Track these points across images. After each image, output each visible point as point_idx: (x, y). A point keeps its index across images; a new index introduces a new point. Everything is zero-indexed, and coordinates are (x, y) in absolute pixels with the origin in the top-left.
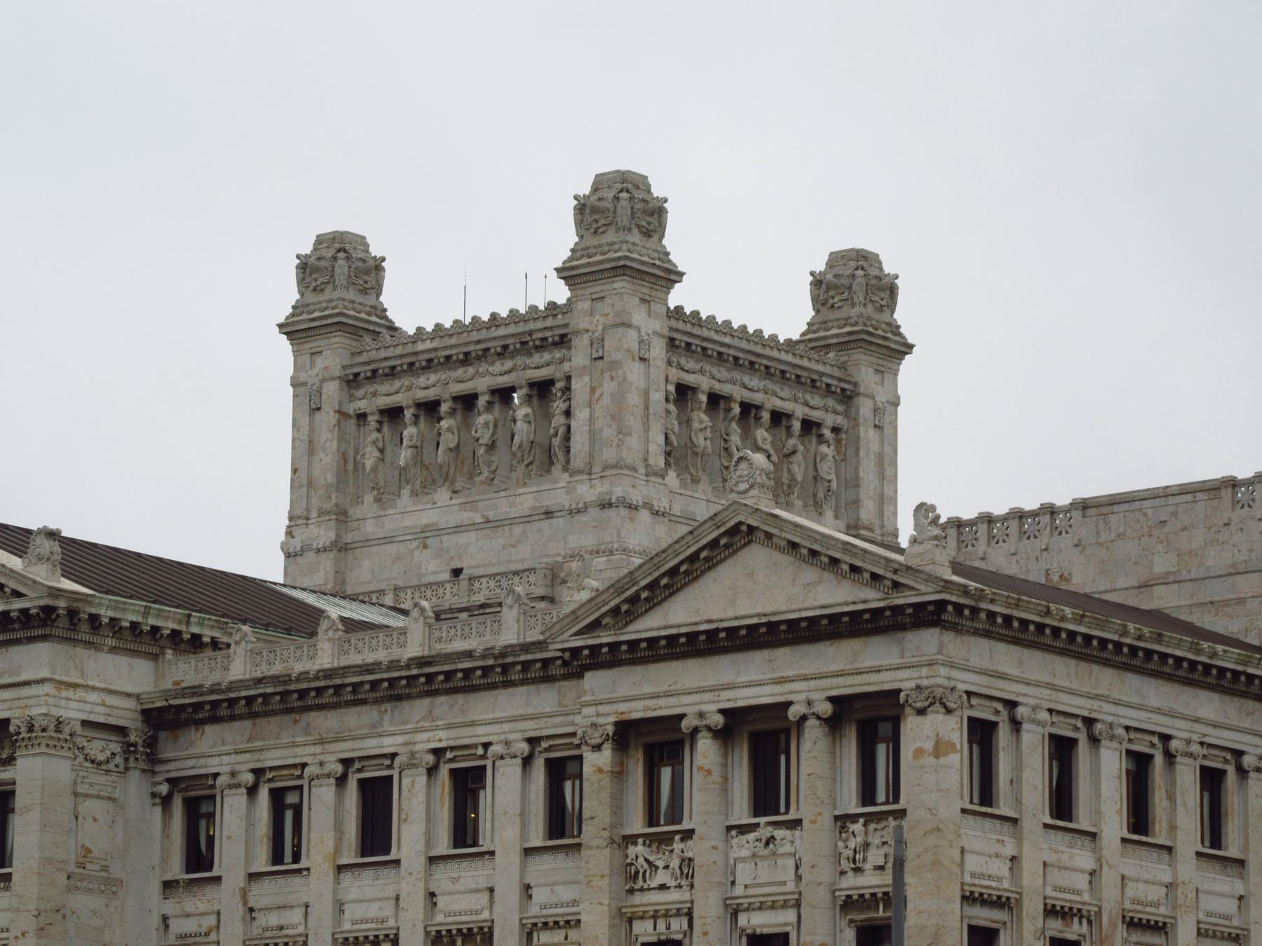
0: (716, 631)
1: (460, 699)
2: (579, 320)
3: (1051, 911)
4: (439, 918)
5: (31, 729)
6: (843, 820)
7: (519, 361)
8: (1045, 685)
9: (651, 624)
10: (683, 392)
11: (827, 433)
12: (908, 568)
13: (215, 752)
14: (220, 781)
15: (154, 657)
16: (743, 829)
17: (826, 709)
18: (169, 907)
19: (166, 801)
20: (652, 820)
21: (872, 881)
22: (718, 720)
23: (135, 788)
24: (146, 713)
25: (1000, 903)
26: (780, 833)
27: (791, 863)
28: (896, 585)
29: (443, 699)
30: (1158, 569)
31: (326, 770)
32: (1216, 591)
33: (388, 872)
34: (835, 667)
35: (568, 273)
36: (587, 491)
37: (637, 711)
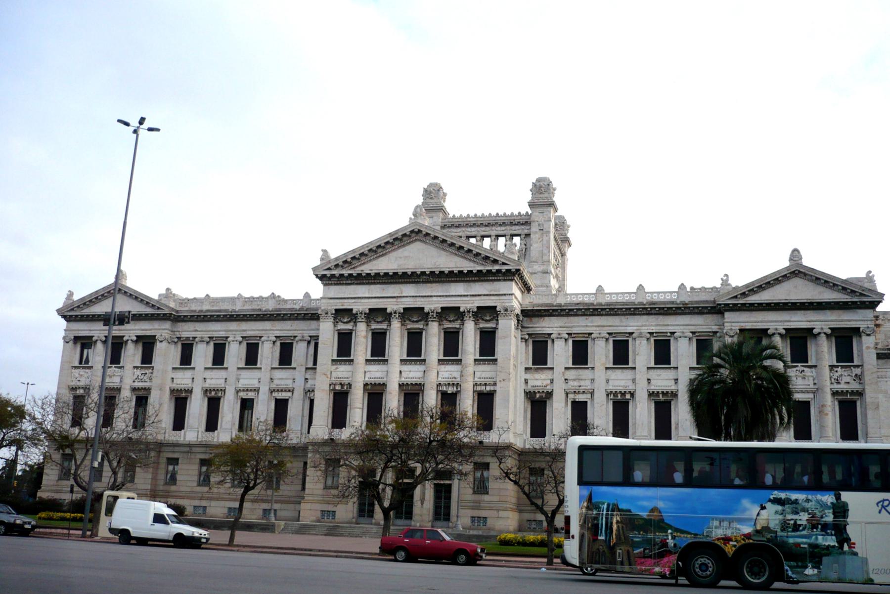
1: (661, 317)
4: (653, 387)
5: (506, 310)
6: (832, 367)
7: (508, 227)
12: (870, 290)
14: (552, 336)
15: (523, 293)
18: (528, 376)
19: (526, 341)
22: (784, 332)
26: (806, 369)
28: (861, 295)
31: (602, 335)
33: (629, 372)
35: (532, 205)
36: (537, 268)
37: (749, 326)
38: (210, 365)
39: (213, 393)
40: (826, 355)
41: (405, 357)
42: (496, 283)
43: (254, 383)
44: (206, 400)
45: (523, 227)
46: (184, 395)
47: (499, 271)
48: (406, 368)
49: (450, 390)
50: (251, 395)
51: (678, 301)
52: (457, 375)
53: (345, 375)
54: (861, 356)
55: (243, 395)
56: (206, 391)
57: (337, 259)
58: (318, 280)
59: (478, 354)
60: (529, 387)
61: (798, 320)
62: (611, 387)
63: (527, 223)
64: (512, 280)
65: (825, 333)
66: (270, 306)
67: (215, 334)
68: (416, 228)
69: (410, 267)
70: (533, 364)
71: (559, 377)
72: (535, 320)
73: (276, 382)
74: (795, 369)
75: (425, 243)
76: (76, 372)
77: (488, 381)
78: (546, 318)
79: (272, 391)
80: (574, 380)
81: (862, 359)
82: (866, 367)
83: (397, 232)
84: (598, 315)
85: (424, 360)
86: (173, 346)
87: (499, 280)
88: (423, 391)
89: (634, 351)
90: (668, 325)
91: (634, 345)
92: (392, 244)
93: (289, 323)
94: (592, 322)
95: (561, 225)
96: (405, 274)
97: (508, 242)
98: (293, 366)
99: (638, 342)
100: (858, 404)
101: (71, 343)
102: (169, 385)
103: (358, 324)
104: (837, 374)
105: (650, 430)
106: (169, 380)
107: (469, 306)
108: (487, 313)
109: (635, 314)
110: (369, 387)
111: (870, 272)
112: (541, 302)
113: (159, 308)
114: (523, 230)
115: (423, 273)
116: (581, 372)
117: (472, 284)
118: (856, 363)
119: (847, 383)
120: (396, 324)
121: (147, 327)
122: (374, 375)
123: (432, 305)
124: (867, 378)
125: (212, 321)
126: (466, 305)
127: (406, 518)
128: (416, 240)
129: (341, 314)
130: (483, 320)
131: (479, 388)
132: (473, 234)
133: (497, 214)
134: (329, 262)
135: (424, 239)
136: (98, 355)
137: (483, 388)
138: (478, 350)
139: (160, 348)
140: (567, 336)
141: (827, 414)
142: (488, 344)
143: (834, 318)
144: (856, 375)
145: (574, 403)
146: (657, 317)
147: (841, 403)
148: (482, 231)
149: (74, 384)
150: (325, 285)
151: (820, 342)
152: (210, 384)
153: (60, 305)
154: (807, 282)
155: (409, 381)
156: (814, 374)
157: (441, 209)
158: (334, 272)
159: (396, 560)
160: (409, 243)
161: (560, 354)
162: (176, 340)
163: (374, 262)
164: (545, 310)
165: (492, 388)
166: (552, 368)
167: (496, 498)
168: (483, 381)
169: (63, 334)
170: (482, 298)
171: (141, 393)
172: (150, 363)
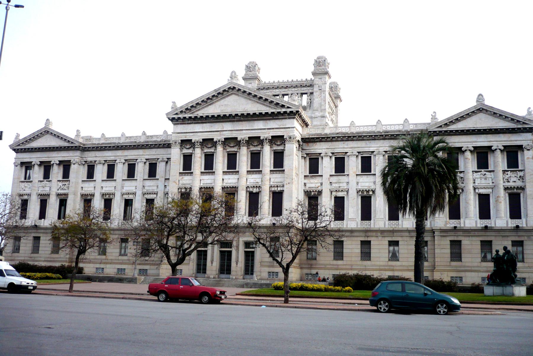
2: (315, 82)
5: (290, 138)
6: (504, 171)
7: (299, 89)
12: (529, 120)
14: (322, 155)
15: (302, 127)
16: (476, 172)
17: (502, 148)
18: (306, 181)
19: (305, 158)
22: (472, 149)
26: (487, 173)
27: (491, 179)
28: (524, 123)
29: (387, 140)
31: (354, 154)
33: (372, 177)
35: (314, 74)
36: (318, 114)
38: (105, 178)
39: (107, 196)
40: (501, 164)
41: (226, 170)
42: (284, 120)
43: (133, 189)
44: (103, 200)
45: (309, 88)
46: (89, 198)
47: (285, 112)
48: (226, 177)
49: (255, 190)
50: (131, 197)
51: (403, 130)
52: (259, 180)
53: (188, 182)
54: (524, 164)
55: (126, 197)
56: (103, 195)
57: (181, 107)
58: (170, 122)
59: (272, 167)
60: (307, 188)
61: (482, 141)
62: (360, 187)
63: (311, 86)
64: (294, 118)
65: (500, 149)
66: (142, 140)
67: (108, 159)
68: (232, 86)
69: (228, 111)
70: (310, 173)
71: (327, 182)
72: (310, 144)
73: (146, 188)
74: (480, 173)
75: (238, 95)
76: (23, 185)
77: (279, 184)
78: (318, 143)
79: (144, 194)
80: (336, 183)
81: (524, 166)
82: (526, 171)
83: (219, 89)
84: (351, 140)
85: (238, 172)
86: (82, 167)
87: (286, 118)
88: (237, 191)
89: (375, 164)
91: (375, 160)
92: (217, 96)
93: (154, 150)
94: (347, 145)
95: (334, 88)
96: (225, 115)
97: (300, 98)
98: (157, 178)
99: (377, 157)
100: (522, 195)
101: (19, 166)
102: (79, 192)
103: (196, 149)
104: (507, 176)
105: (385, 215)
106: (80, 188)
107: (266, 136)
108: (278, 140)
109: (375, 139)
110: (203, 190)
111: (530, 108)
112: (314, 133)
113: (72, 143)
115: (237, 115)
116: (340, 177)
117: (268, 121)
118: (520, 168)
119: (514, 181)
120: (220, 148)
121: (65, 155)
122: (206, 182)
123: (243, 136)
124: (527, 178)
125: (106, 150)
126: (264, 135)
127: (227, 274)
128: (232, 94)
129: (185, 143)
130: (275, 144)
131: (273, 189)
132: (277, 93)
133: (292, 80)
134: (177, 109)
135: (237, 93)
136: (37, 173)
137: (276, 189)
138: (272, 164)
139: (74, 168)
140: (331, 155)
141: (501, 202)
142: (279, 160)
143: (506, 139)
144: (520, 176)
145: (336, 198)
146: (390, 141)
147: (510, 195)
148: (283, 91)
149: (22, 192)
150: (174, 124)
151: (497, 155)
152: (106, 190)
153: (12, 142)
154: (487, 116)
155: (228, 185)
156: (493, 176)
157: (256, 78)
158: (179, 116)
159: (159, 301)
160: (227, 96)
161: (327, 166)
162: (84, 163)
163: (206, 109)
164: (317, 138)
165: (282, 189)
166: (322, 176)
168: (276, 184)
169: (14, 161)
170: (275, 130)
171: (62, 197)
172: (68, 178)
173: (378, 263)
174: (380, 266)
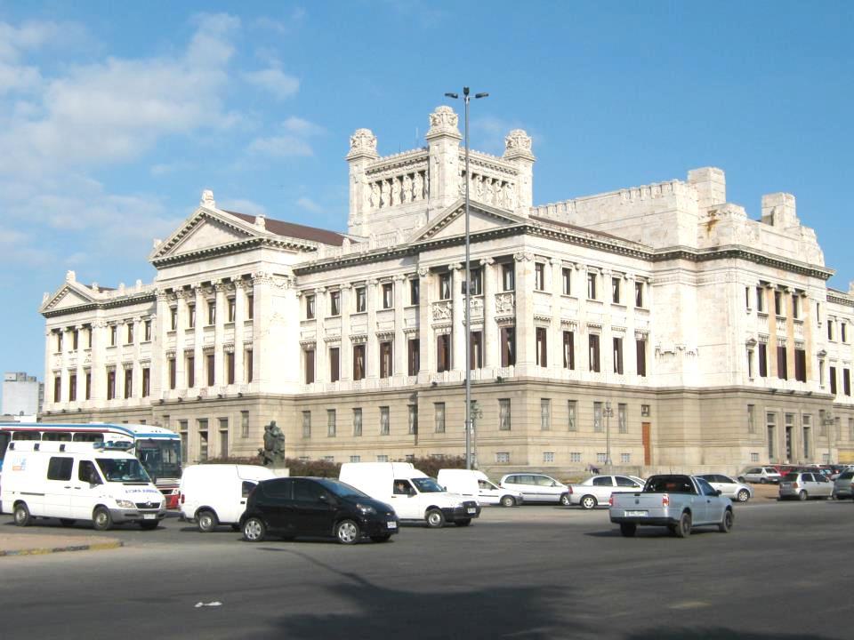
0: (457, 238)
3: (563, 323)
6: (498, 295)
7: (416, 165)
8: (561, 252)
9: (439, 237)
10: (464, 173)
11: (510, 185)
13: (314, 281)
17: (492, 261)
19: (300, 297)
20: (441, 298)
21: (506, 314)
22: (460, 266)
23: (292, 293)
24: (294, 271)
25: (547, 320)
28: (512, 222)
30: (602, 218)
31: (346, 286)
32: (619, 224)
34: (494, 248)
37: (435, 264)
49: (231, 350)
69: (203, 246)
72: (305, 277)
78: (312, 275)
90: (388, 270)
114: (423, 166)
161: (323, 304)
163: (185, 245)
167: (253, 441)
173: (369, 439)
174: (371, 442)
